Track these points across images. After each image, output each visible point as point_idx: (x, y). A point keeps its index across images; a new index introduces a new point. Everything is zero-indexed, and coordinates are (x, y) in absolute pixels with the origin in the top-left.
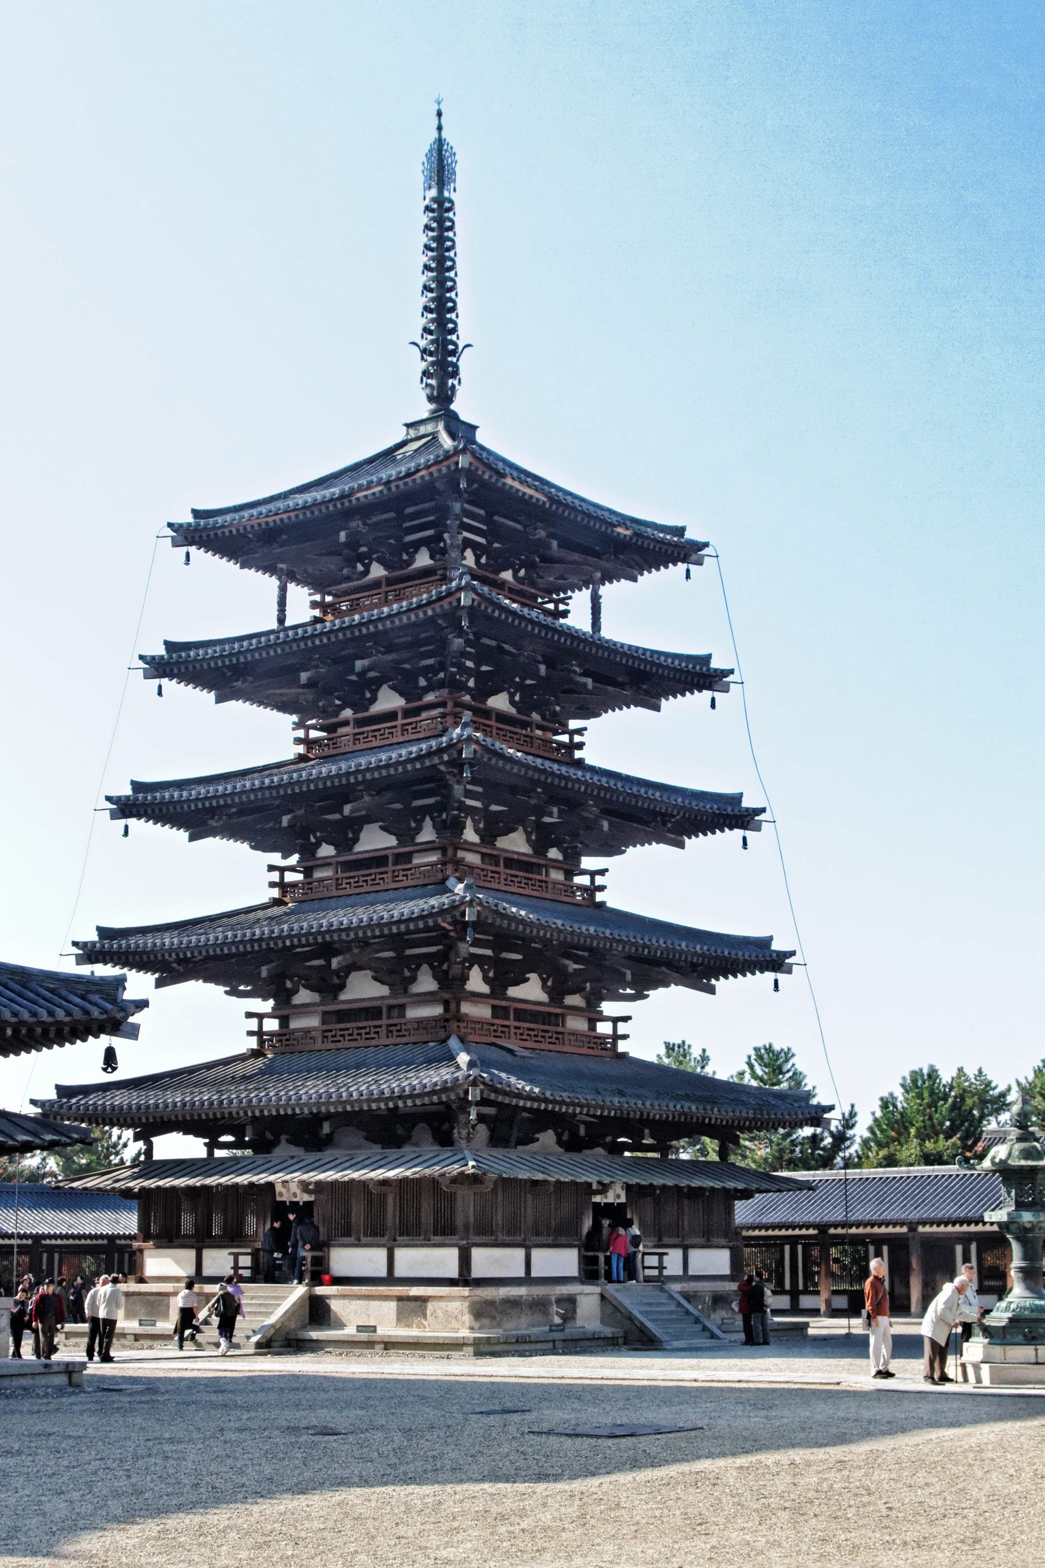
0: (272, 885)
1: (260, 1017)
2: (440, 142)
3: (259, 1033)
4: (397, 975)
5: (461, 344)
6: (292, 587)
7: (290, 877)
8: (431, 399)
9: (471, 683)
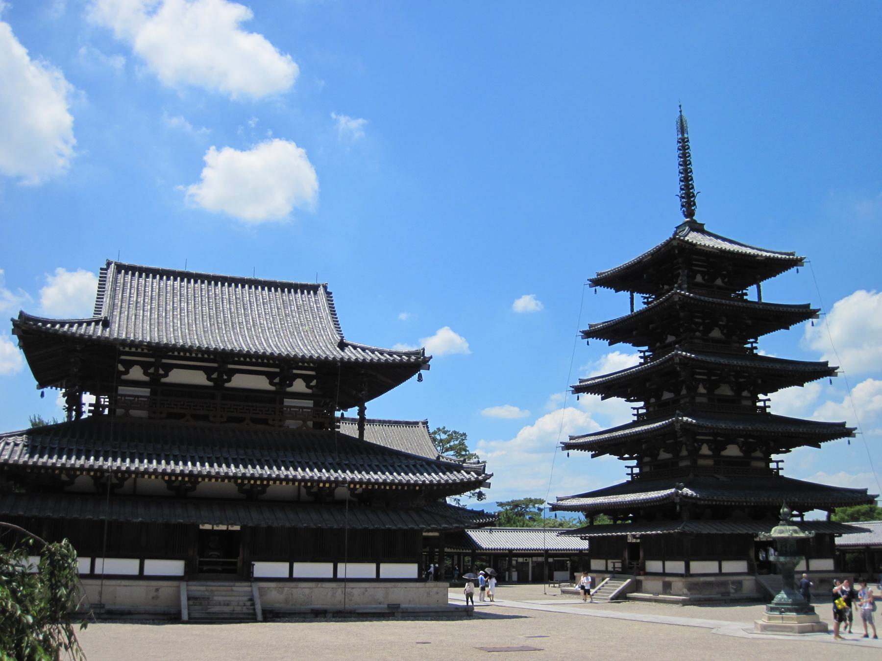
0: (634, 415)
1: (632, 468)
2: (681, 116)
3: (632, 474)
4: (674, 449)
5: (695, 193)
6: (635, 294)
9: (701, 328)
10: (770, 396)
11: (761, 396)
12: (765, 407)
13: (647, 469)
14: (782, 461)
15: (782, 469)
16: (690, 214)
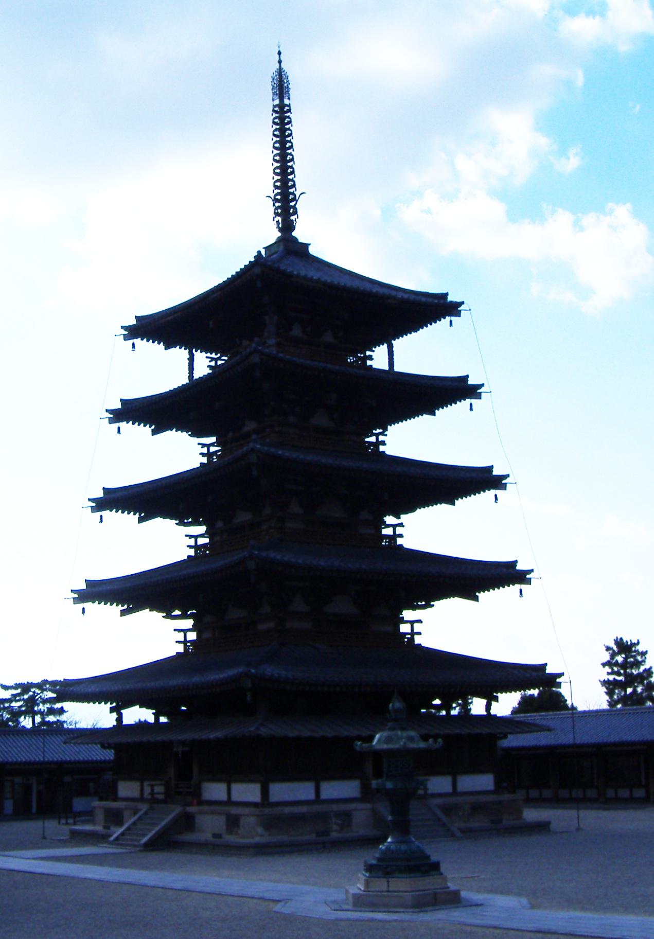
0: (190, 547)
1: (185, 631)
5: (298, 194)
7: (202, 541)
8: (280, 230)
10: (404, 518)
11: (390, 519)
12: (395, 536)
13: (207, 635)
14: (420, 621)
15: (419, 633)
16: (287, 227)
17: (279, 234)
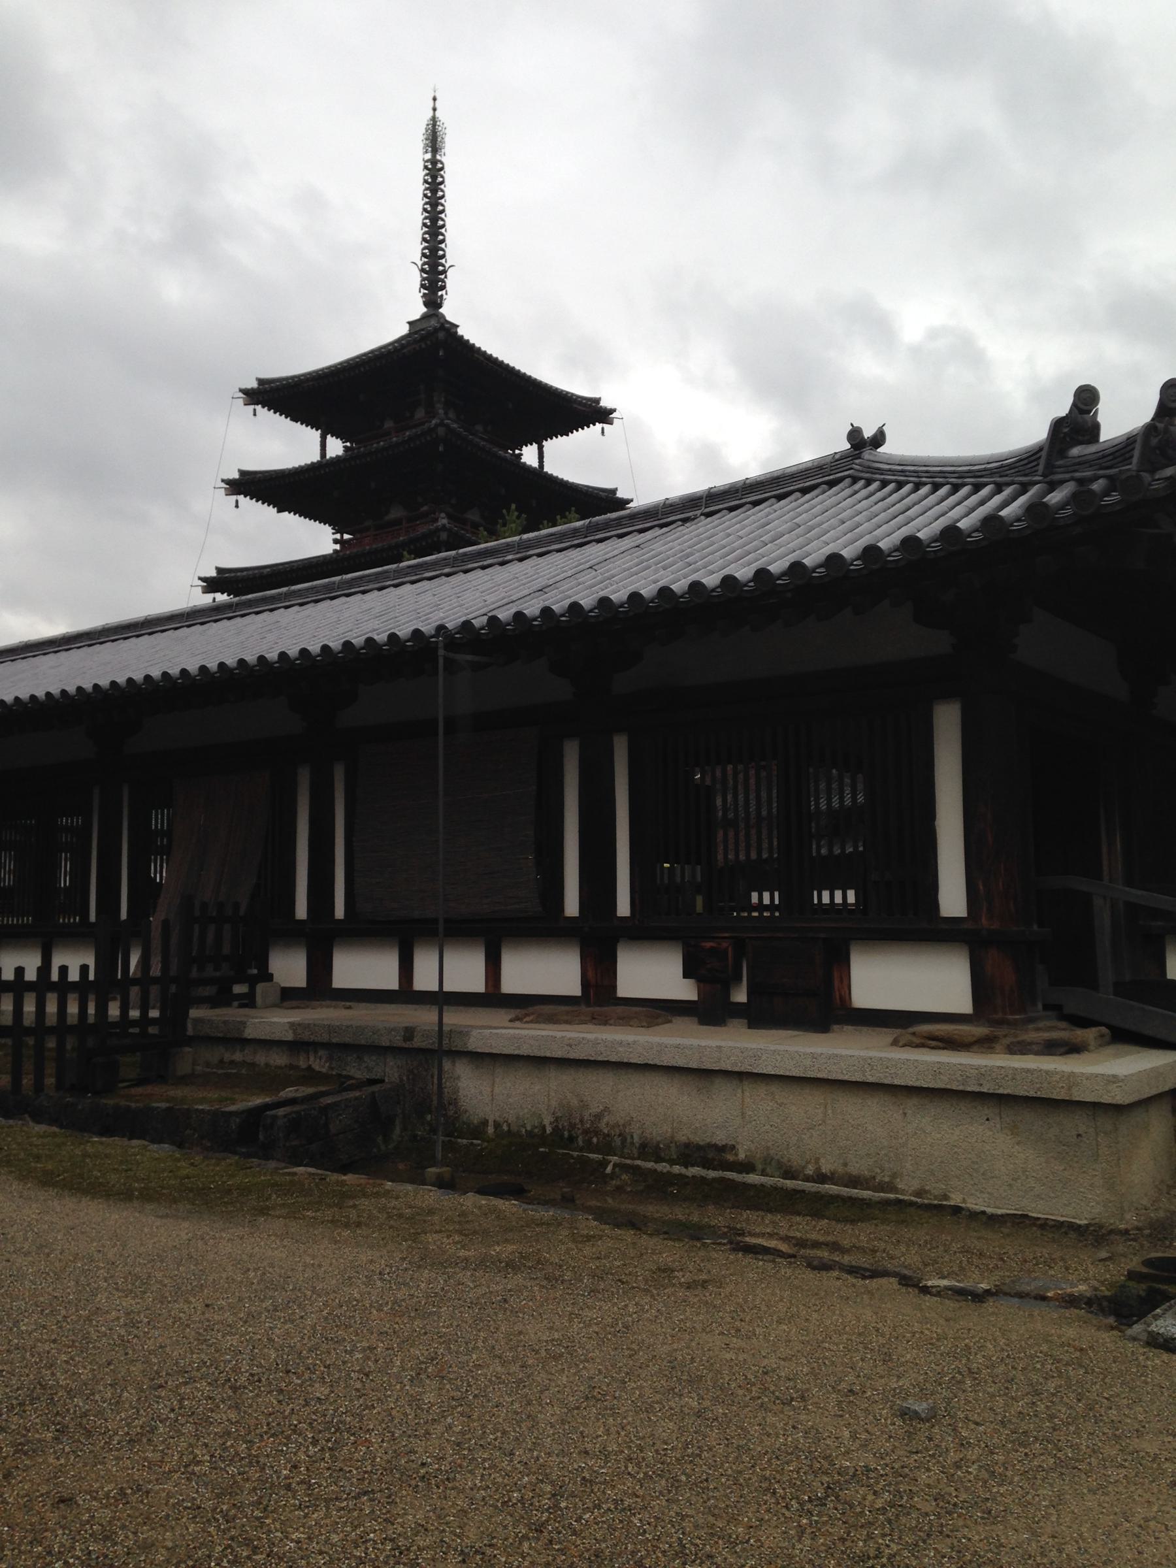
2: (434, 120)
5: (447, 266)
8: (426, 304)
9: (453, 501)
17: (424, 310)
